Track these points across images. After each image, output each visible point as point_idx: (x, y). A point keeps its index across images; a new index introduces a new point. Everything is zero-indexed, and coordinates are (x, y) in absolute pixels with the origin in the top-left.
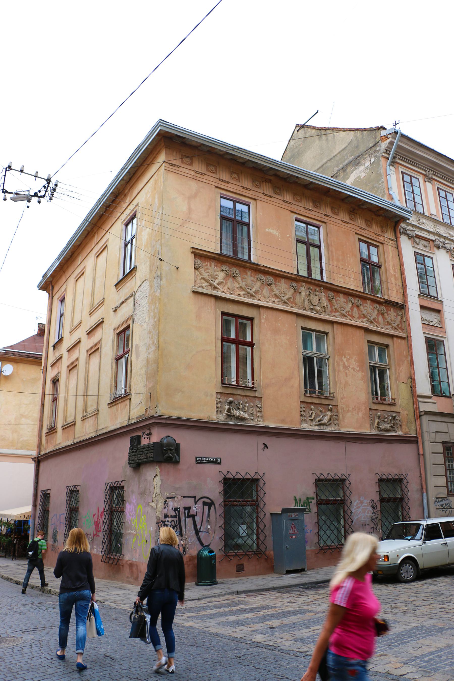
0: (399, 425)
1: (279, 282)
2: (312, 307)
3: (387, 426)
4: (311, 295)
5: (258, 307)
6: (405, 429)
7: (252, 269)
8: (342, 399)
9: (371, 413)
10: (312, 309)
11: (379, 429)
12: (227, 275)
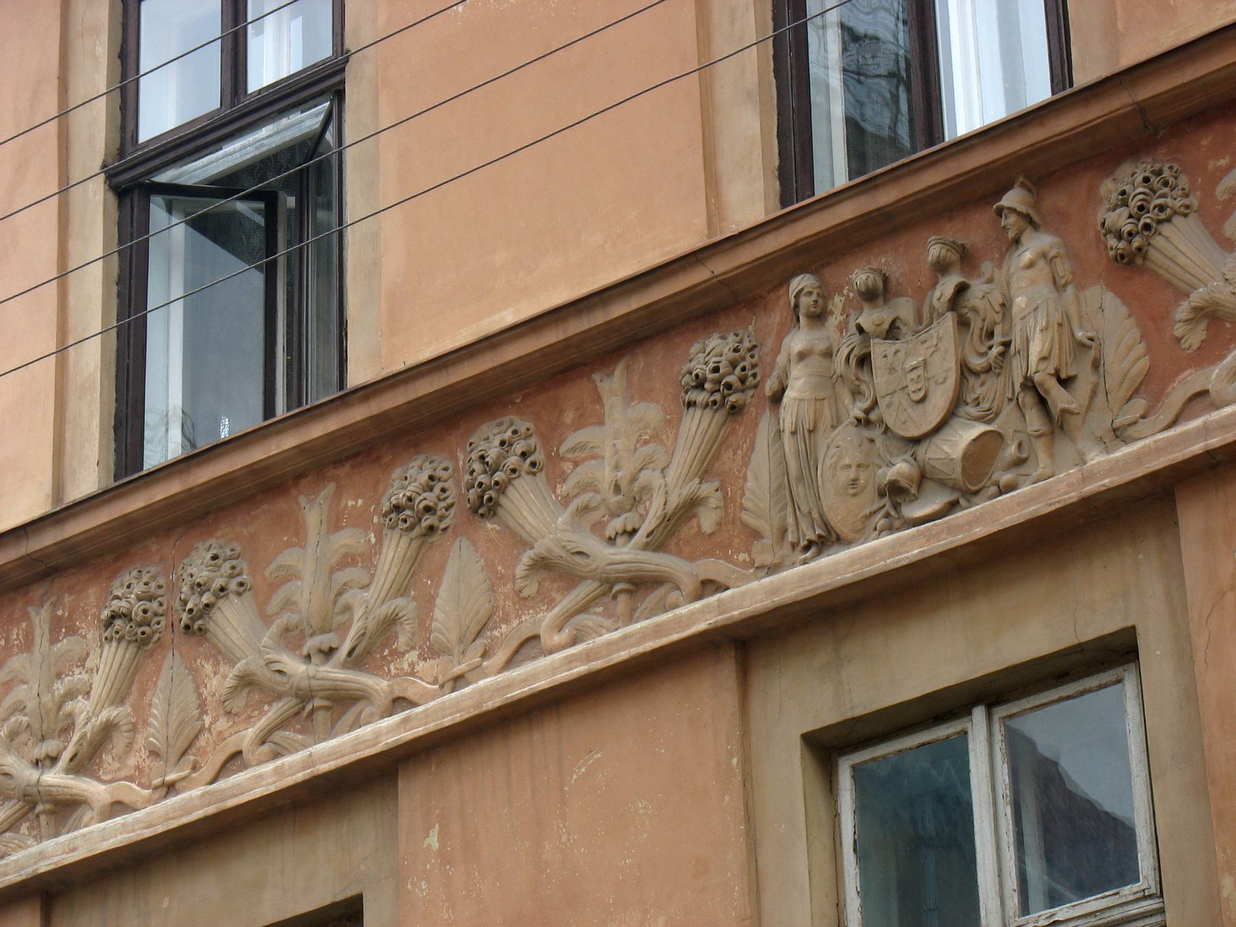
1: (579, 424)
2: (901, 468)
4: (879, 349)
5: (367, 782)
7: (338, 462)
10: (895, 492)
12: (142, 642)
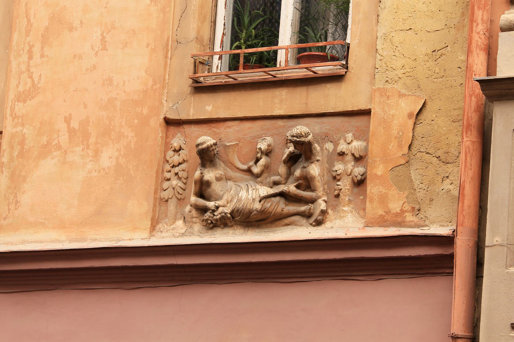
0: (345, 184)
3: (250, 195)
6: (383, 200)
8: (22, 98)
9: (176, 143)
11: (208, 214)
